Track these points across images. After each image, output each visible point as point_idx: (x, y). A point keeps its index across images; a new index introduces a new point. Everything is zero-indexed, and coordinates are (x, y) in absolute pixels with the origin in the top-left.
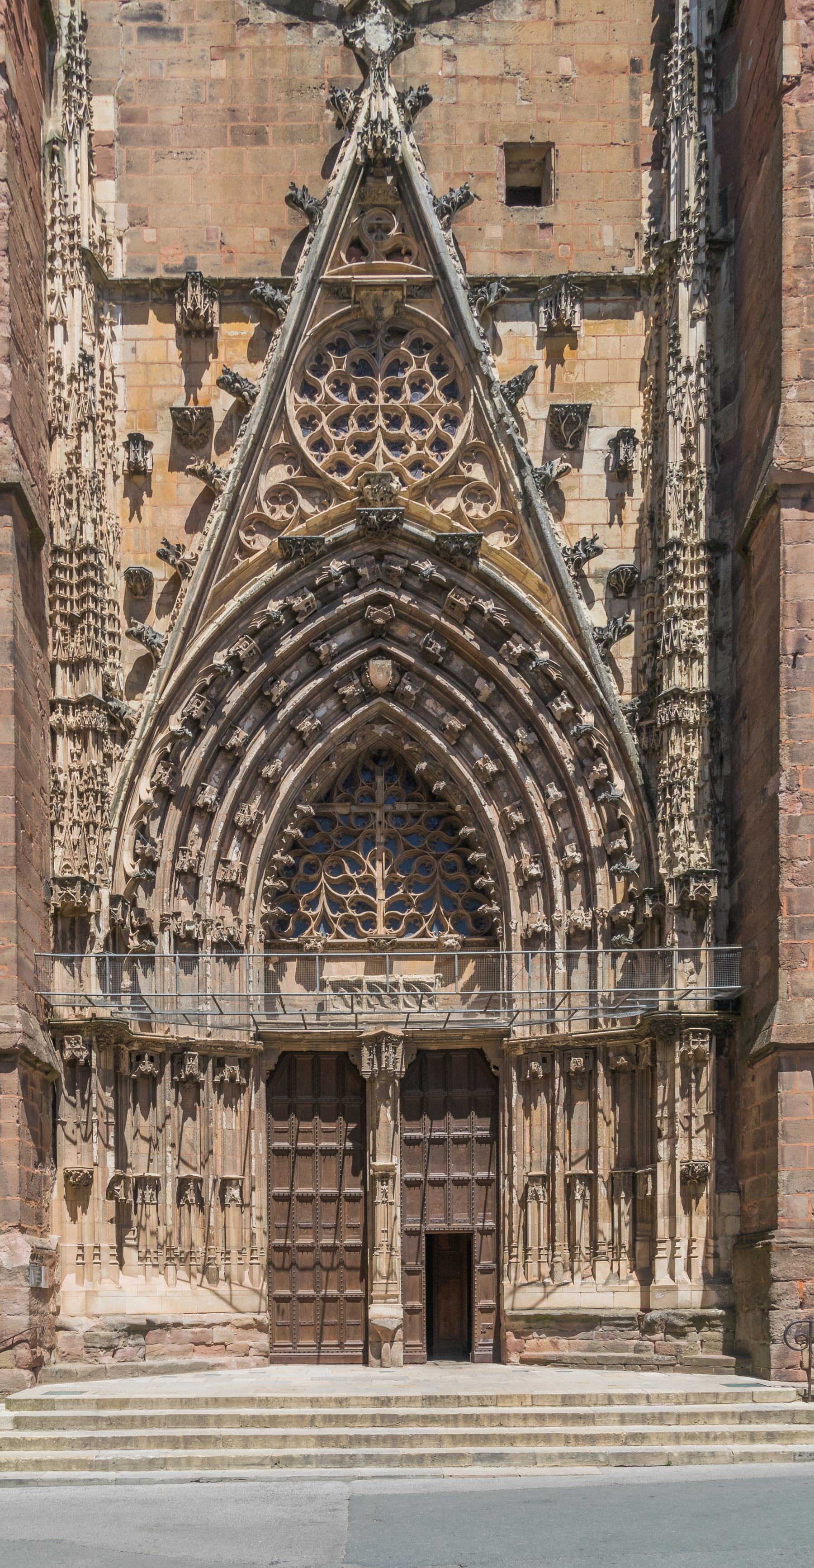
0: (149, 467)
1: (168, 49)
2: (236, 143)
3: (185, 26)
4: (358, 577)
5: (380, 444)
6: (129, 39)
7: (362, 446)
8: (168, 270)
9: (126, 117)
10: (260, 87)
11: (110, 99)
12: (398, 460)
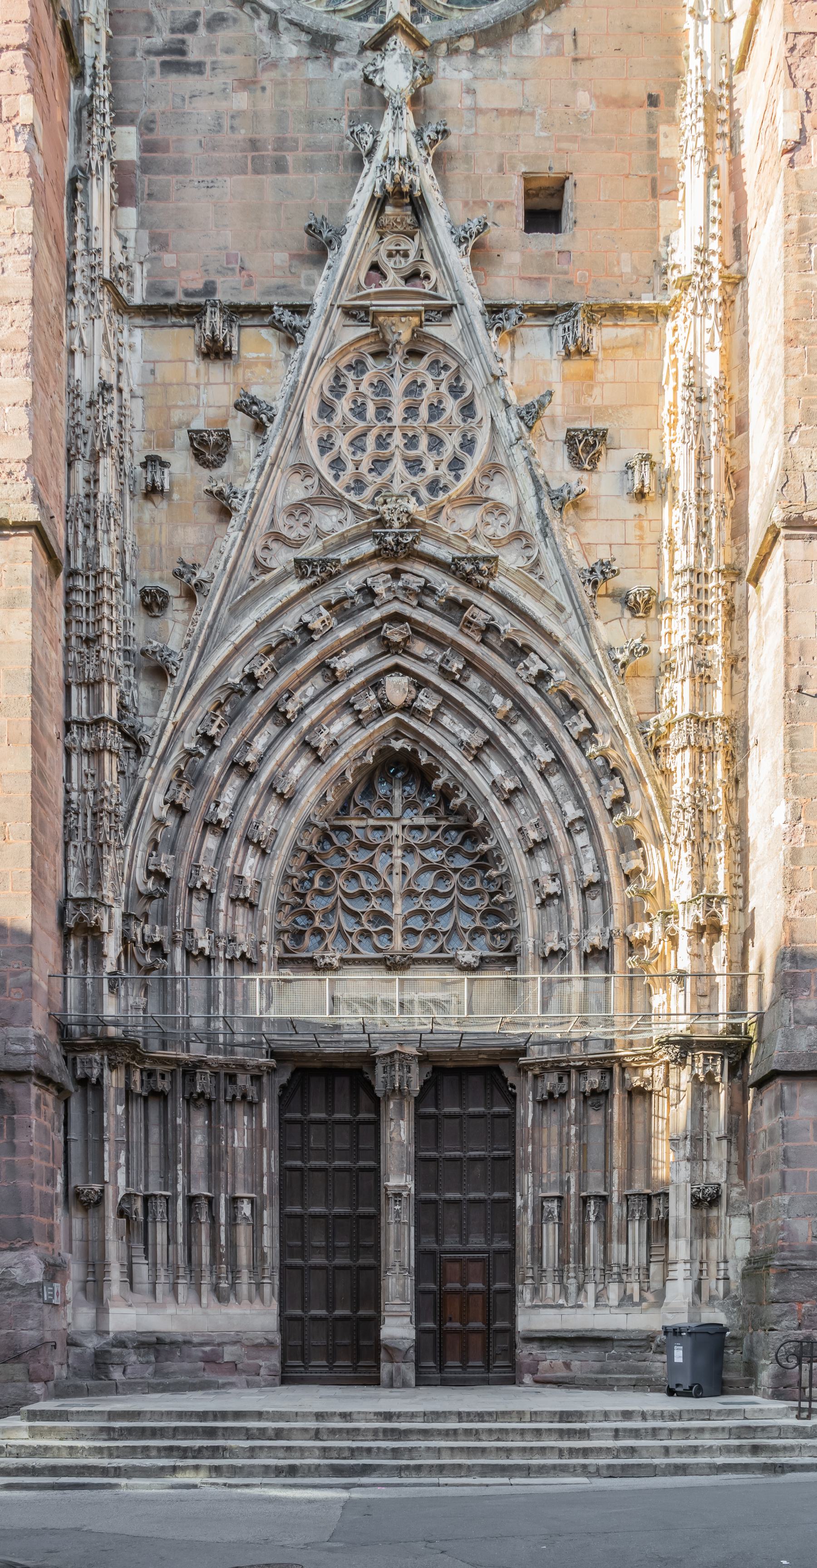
0: (167, 486)
1: (190, 82)
2: (256, 172)
3: (208, 59)
4: (374, 595)
5: (397, 466)
6: (152, 72)
7: (380, 464)
8: (187, 294)
9: (147, 147)
10: (281, 118)
11: (133, 129)
12: (415, 480)
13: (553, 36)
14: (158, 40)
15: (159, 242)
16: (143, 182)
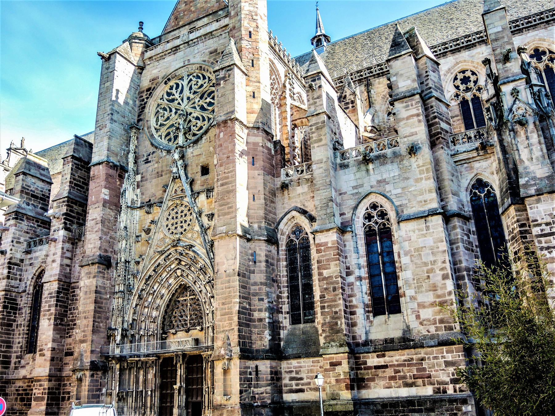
9: (142, 178)
10: (162, 167)
13: (207, 139)
14: (145, 159)
15: (142, 194)
16: (141, 184)
